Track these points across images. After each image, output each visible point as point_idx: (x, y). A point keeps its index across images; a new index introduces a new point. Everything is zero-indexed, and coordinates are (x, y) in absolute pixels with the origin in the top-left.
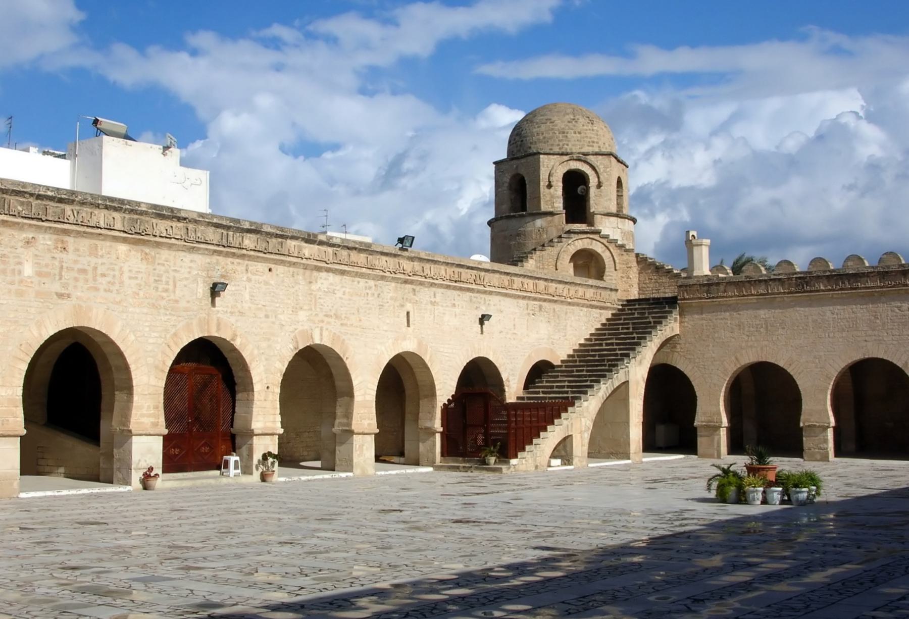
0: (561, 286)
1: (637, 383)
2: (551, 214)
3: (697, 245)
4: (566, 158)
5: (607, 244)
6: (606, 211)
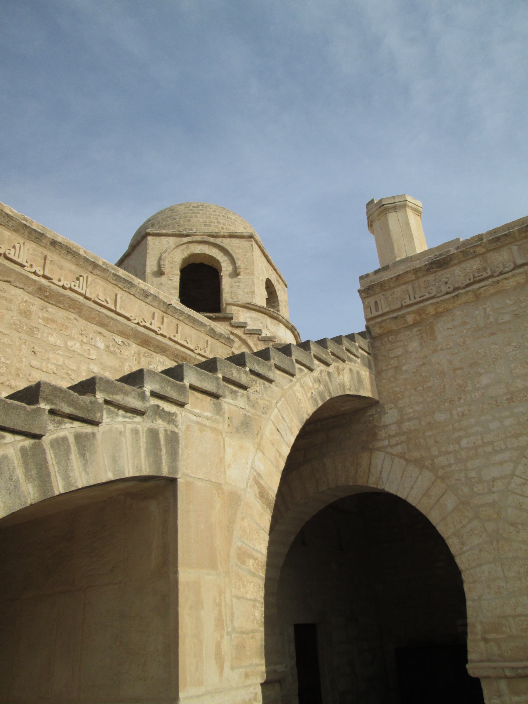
1: (234, 500)
4: (185, 240)
5: (244, 337)
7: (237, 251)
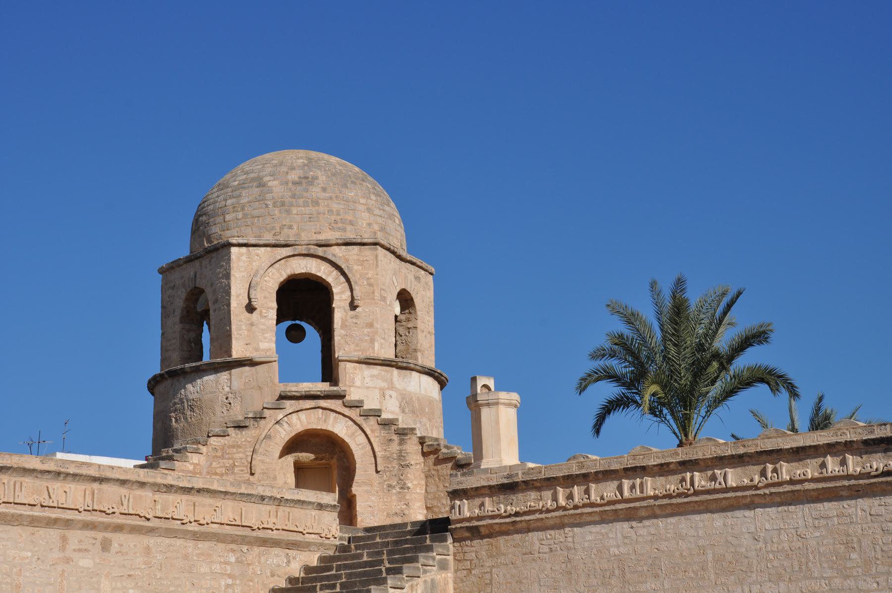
0: (171, 497)
2: (251, 363)
3: (488, 405)
5: (360, 420)
6: (362, 356)
7: (356, 267)
